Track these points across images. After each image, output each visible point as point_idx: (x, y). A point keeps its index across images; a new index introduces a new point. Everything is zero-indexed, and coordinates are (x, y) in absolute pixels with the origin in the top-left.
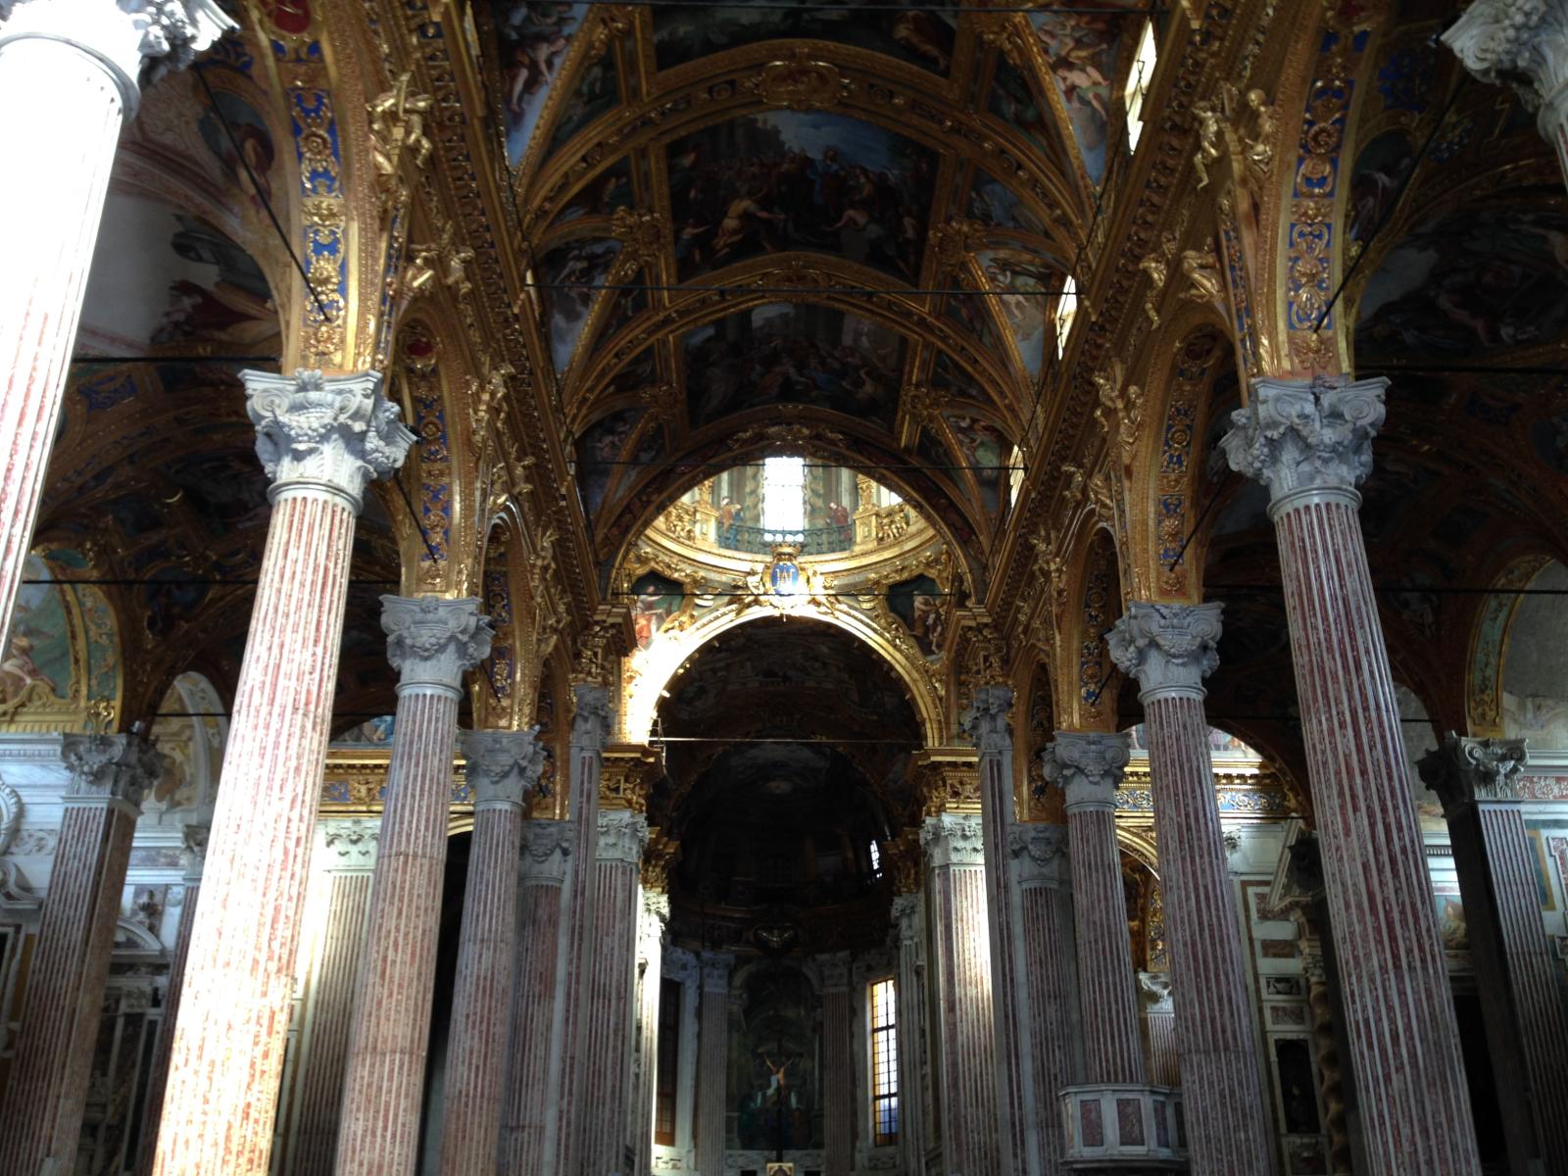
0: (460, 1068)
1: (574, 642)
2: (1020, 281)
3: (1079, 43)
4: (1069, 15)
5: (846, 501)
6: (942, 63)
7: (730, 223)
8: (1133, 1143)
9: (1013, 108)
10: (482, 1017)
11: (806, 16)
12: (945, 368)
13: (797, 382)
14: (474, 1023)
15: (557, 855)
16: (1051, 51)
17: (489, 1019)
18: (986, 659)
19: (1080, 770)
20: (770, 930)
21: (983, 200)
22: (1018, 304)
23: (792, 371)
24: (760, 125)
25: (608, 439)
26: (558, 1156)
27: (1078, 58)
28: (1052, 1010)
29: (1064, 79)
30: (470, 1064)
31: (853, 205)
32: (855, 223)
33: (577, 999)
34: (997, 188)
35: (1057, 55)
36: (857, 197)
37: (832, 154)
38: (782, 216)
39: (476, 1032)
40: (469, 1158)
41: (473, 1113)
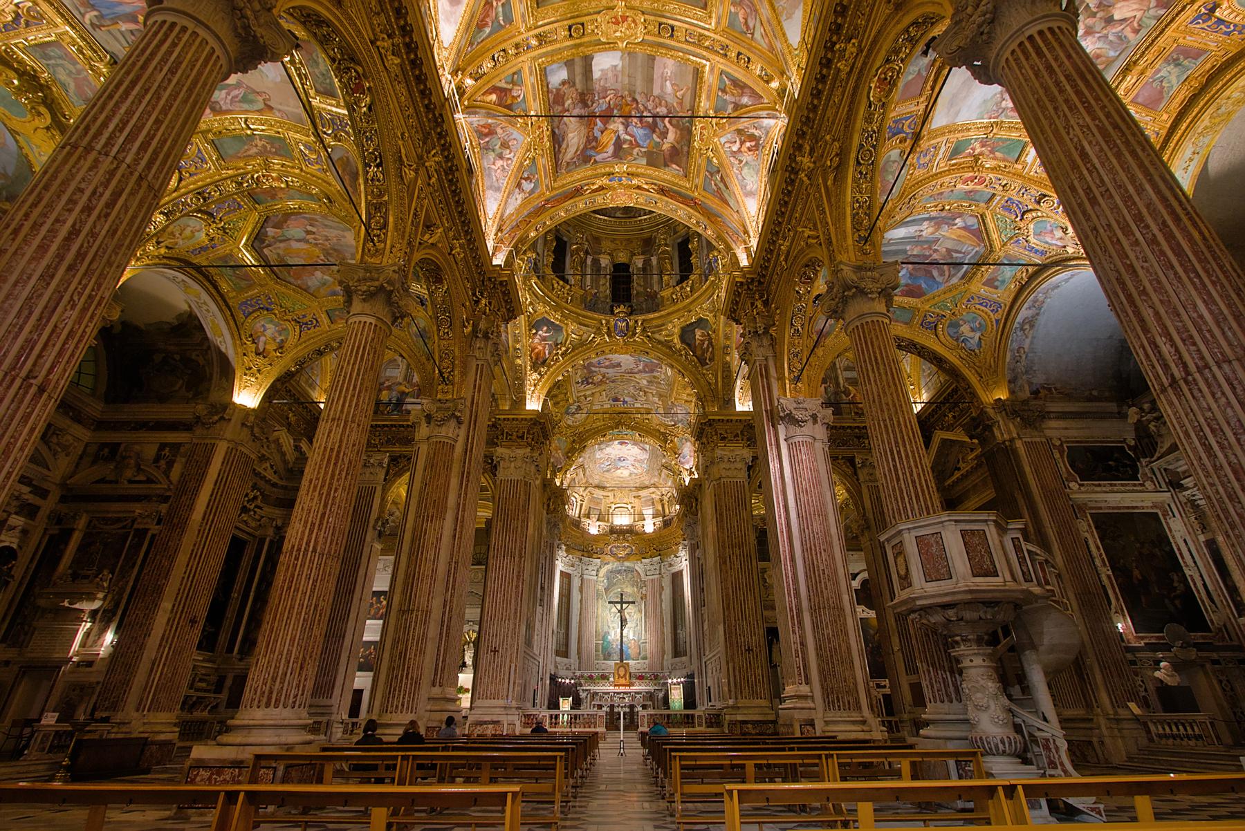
0: (297, 525)
1: (474, 294)
5: (656, 288)
8: (986, 574)
10: (324, 481)
12: (724, 91)
13: (625, 141)
14: (315, 487)
15: (453, 423)
17: (331, 484)
18: (752, 304)
19: (862, 292)
20: (618, 547)
23: (621, 128)
25: (499, 163)
26: (441, 634)
28: (816, 524)
30: (306, 522)
33: (462, 522)
39: (316, 494)
40: (292, 607)
41: (303, 565)
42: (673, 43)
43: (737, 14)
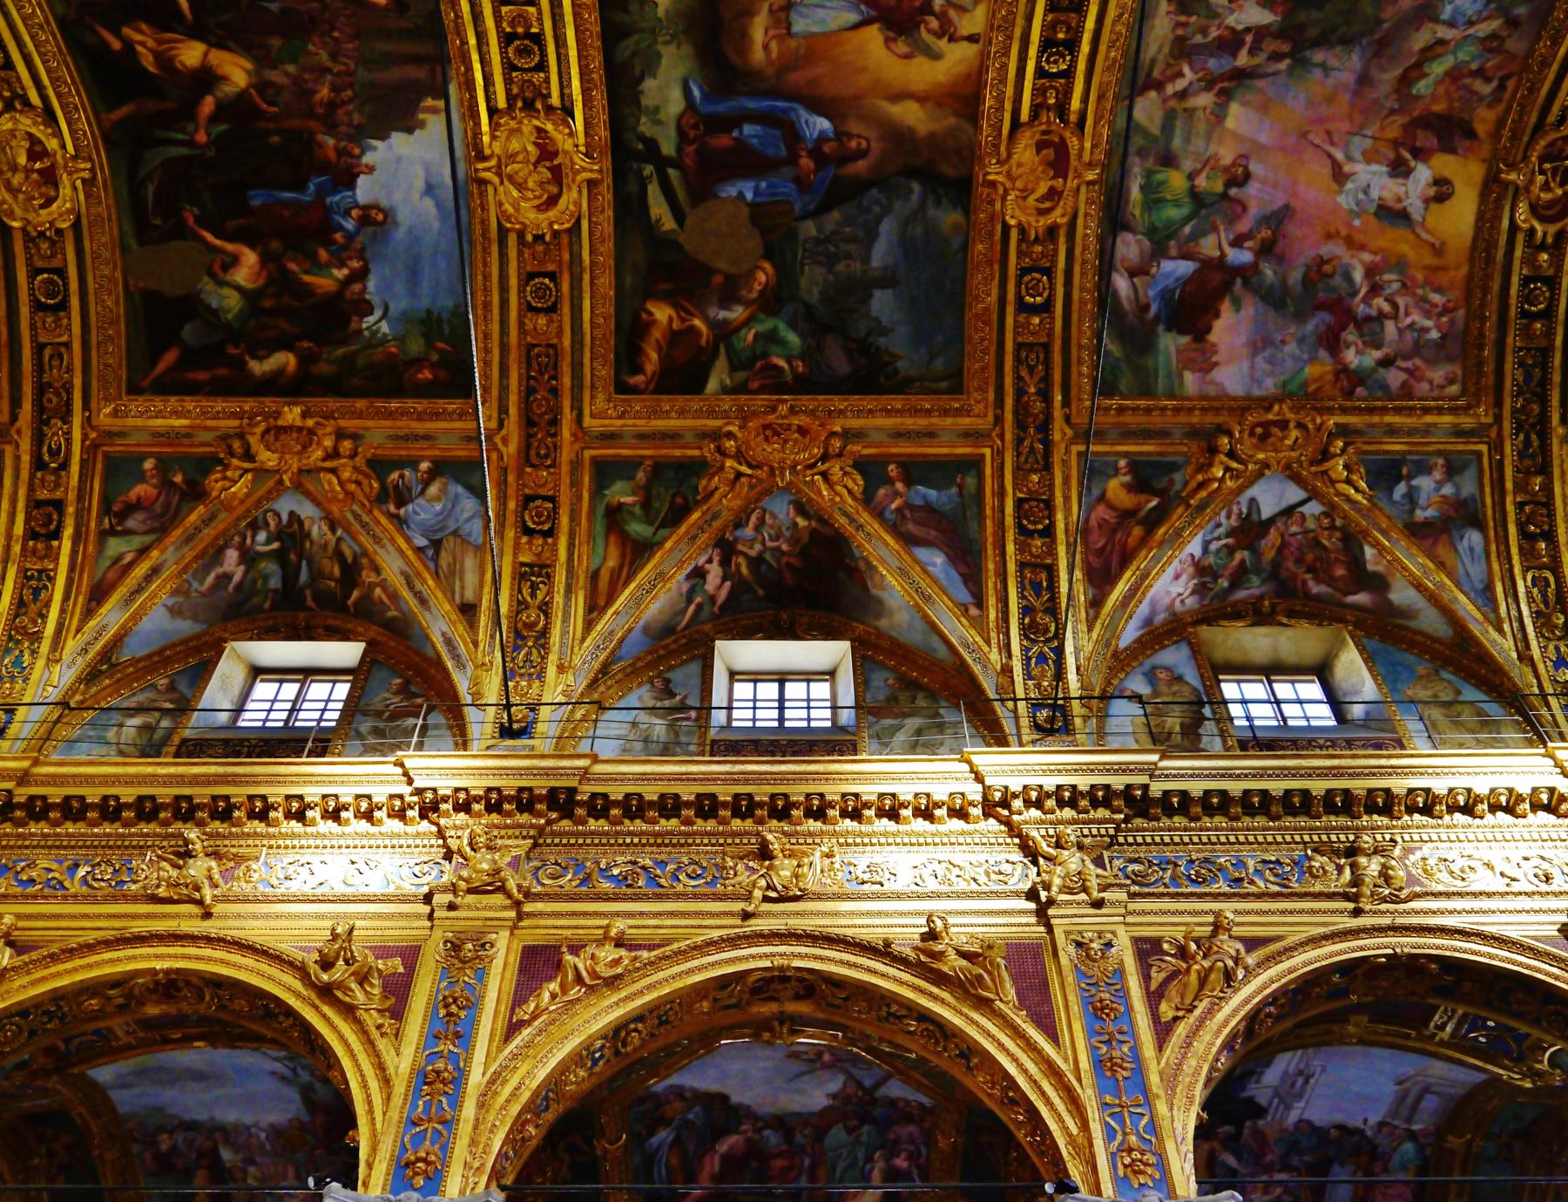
2: (271, 567)
3: (756, 562)
4: (794, 541)
6: (639, 379)
7: (191, 54)
9: (629, 499)
11: (648, 169)
16: (738, 533)
21: (426, 484)
22: (227, 577)
24: (429, 102)
27: (738, 565)
29: (710, 561)
31: (266, 259)
32: (226, 268)
34: (469, 504)
35: (736, 540)
36: (293, 266)
37: (376, 219)
38: (202, 137)
42: (25, 311)
43: (141, 478)
